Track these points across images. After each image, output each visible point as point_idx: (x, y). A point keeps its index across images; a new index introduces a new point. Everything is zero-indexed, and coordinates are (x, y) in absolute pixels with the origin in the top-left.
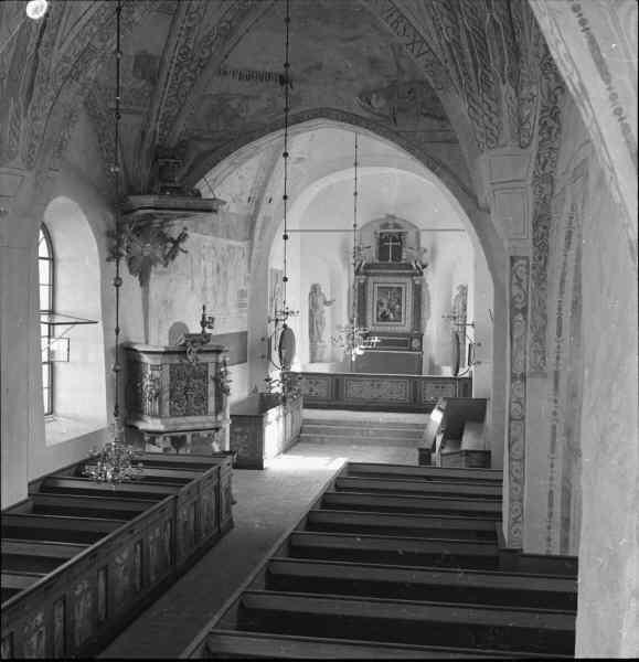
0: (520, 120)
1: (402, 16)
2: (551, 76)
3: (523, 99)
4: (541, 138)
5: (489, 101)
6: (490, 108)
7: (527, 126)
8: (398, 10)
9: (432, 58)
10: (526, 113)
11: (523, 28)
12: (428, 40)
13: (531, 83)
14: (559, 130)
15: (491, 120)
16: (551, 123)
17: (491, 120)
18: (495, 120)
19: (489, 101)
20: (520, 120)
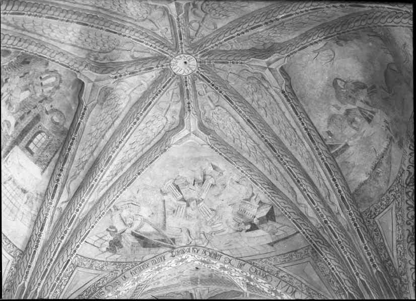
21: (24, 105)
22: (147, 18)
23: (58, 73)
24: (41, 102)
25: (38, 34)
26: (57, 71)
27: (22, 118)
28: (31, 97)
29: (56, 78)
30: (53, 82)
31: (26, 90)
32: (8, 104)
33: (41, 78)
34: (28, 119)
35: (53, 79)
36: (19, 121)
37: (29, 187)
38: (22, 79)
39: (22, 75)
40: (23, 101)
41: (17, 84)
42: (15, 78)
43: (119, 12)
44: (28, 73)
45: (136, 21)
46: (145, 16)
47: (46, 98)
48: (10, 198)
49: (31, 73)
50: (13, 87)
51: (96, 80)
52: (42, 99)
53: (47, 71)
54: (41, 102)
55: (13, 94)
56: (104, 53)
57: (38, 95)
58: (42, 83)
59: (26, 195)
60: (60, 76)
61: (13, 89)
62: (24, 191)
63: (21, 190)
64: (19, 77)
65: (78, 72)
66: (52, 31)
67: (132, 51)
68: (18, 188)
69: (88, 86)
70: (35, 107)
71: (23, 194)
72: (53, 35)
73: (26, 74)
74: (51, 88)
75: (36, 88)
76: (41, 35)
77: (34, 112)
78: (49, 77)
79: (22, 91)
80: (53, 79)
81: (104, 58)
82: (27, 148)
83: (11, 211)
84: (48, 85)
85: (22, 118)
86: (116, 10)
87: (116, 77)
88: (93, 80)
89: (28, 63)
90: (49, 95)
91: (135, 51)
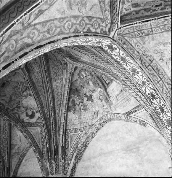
0: (64, 168)
1: (34, 139)
2: (76, 160)
3: (66, 164)
4: (71, 173)
5: (57, 163)
6: (57, 164)
7: (66, 170)
8: (33, 137)
9: (39, 150)
10: (66, 167)
11: (68, 148)
12: (39, 146)
13: (68, 161)
14: (75, 172)
15: (57, 167)
16: (74, 170)
17: (57, 167)
18: (58, 168)
19: (57, 163)
20: (64, 168)
21: (94, 84)
22: (36, 62)
23: (79, 73)
24: (92, 76)
25: (61, 96)
26: (78, 74)
27: (99, 85)
28: (91, 80)
29: (81, 72)
30: (84, 72)
31: (89, 82)
32: (94, 92)
33: (83, 78)
34: (99, 82)
35: (83, 73)
36: (100, 86)
37: (120, 89)
38: (84, 87)
39: (83, 88)
40: (93, 84)
41: (86, 88)
42: (84, 91)
43: (40, 75)
44: (81, 85)
45: (40, 66)
46: (36, 64)
47: (91, 74)
48: (123, 98)
49: (81, 84)
50: (88, 90)
51: (71, 64)
52: (91, 76)
53: (80, 77)
54: (92, 76)
55: (90, 89)
56: (61, 63)
57: (90, 77)
58: (86, 77)
59: (123, 90)
60: (80, 70)
61: (88, 90)
62: (122, 91)
63: (121, 93)
64: (84, 89)
65: (70, 74)
66: (59, 92)
67: (52, 54)
68: (120, 94)
69: (75, 66)
70: (94, 78)
71: (123, 92)
72: (60, 91)
73: (82, 87)
74: (86, 72)
75: (88, 78)
76: (62, 95)
77: (96, 79)
78: (82, 75)
79: (89, 85)
80: (83, 73)
81: (63, 61)
82: (108, 84)
83: (127, 100)
84: (85, 74)
85: (99, 85)
86: (40, 77)
87: (65, 58)
88: (72, 65)
89: (76, 89)
90: (89, 73)
91: (52, 53)
